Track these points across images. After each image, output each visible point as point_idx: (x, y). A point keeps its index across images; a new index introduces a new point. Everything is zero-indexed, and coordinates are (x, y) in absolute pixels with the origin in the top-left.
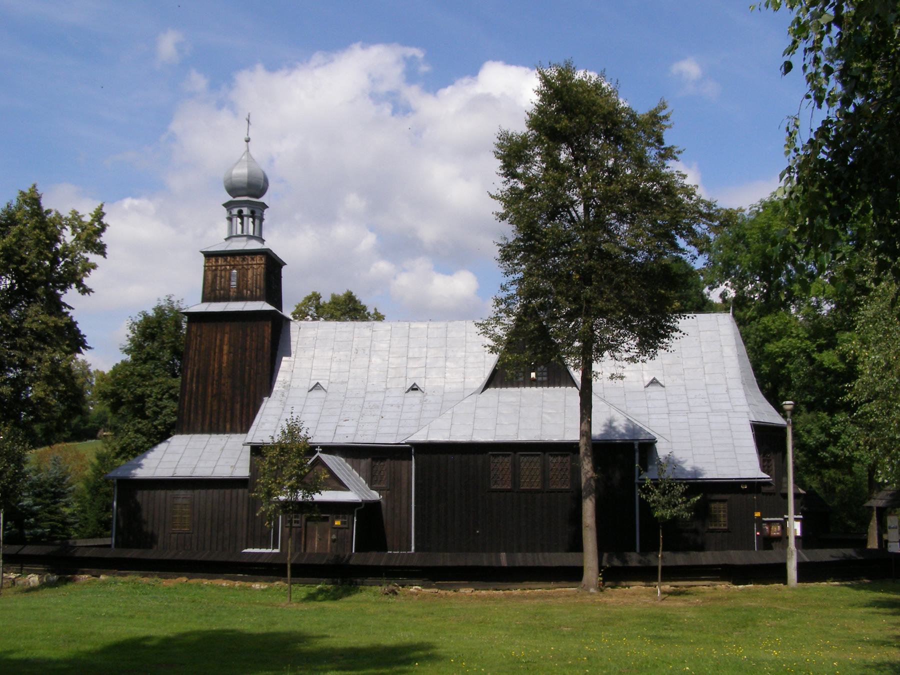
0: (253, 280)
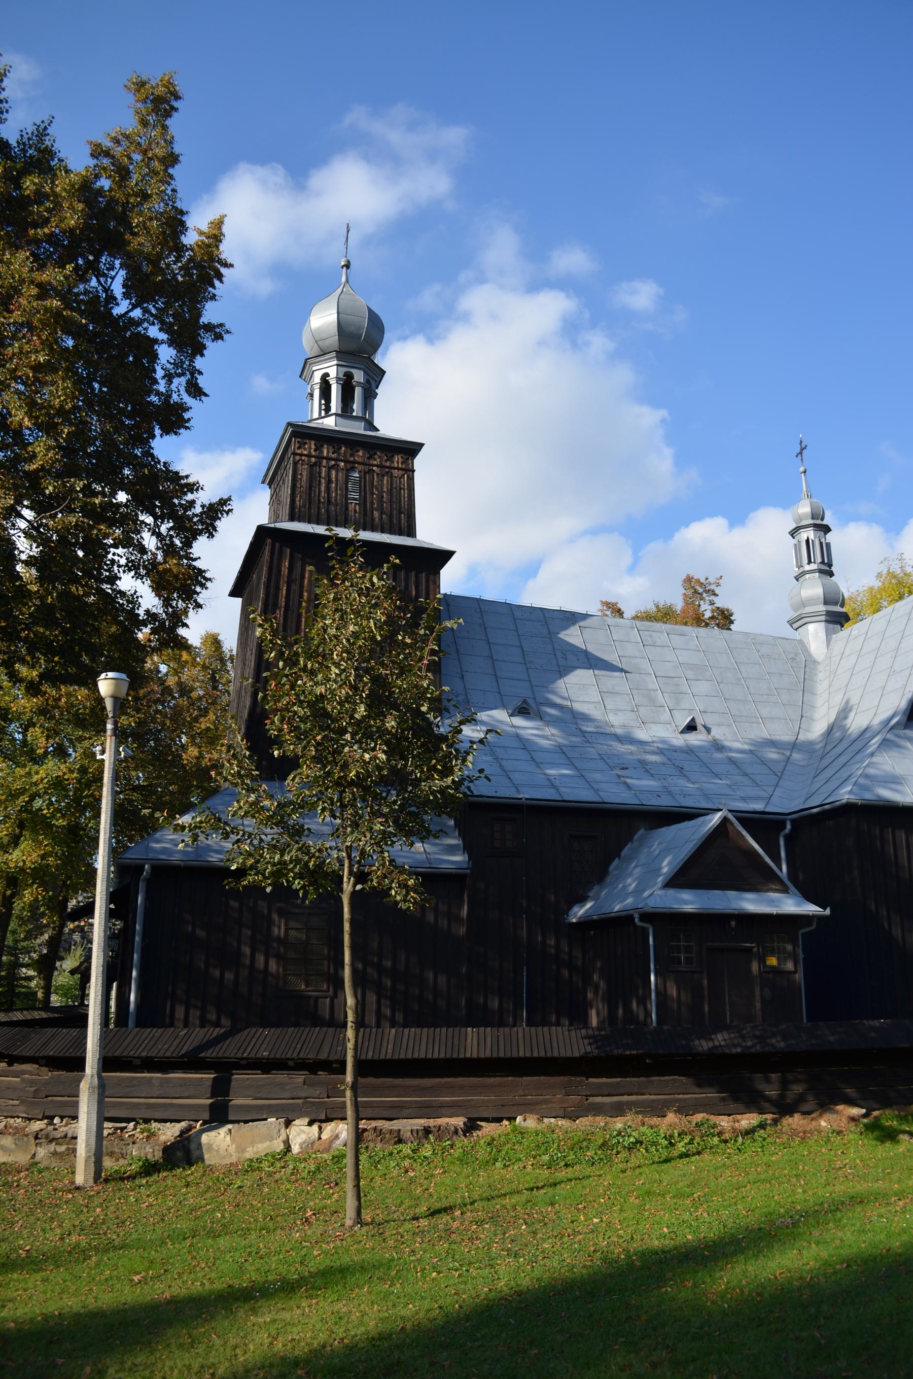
0: (391, 495)
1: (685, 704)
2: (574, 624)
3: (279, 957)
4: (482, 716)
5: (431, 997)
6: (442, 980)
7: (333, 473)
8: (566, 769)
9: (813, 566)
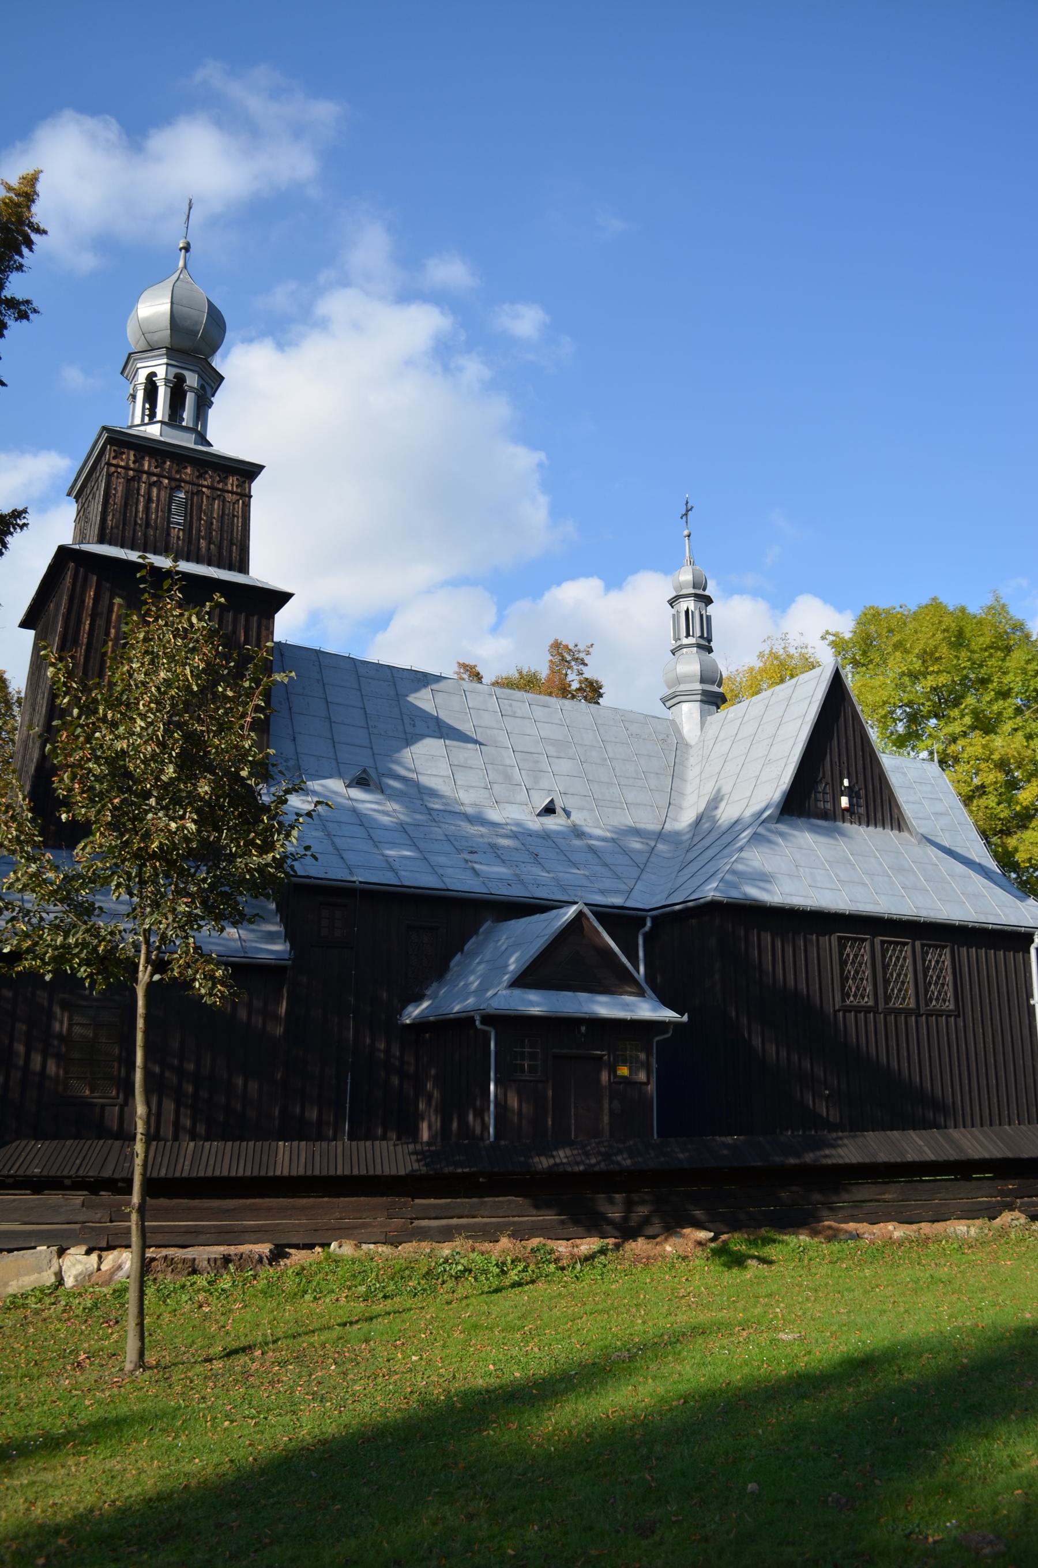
0: (222, 523)
1: (545, 784)
2: (425, 686)
3: (59, 1057)
4: (314, 785)
5: (239, 1107)
6: (253, 1086)
7: (155, 491)
8: (407, 850)
9: (691, 640)
